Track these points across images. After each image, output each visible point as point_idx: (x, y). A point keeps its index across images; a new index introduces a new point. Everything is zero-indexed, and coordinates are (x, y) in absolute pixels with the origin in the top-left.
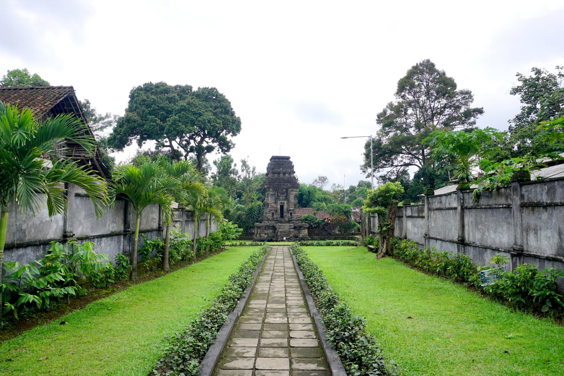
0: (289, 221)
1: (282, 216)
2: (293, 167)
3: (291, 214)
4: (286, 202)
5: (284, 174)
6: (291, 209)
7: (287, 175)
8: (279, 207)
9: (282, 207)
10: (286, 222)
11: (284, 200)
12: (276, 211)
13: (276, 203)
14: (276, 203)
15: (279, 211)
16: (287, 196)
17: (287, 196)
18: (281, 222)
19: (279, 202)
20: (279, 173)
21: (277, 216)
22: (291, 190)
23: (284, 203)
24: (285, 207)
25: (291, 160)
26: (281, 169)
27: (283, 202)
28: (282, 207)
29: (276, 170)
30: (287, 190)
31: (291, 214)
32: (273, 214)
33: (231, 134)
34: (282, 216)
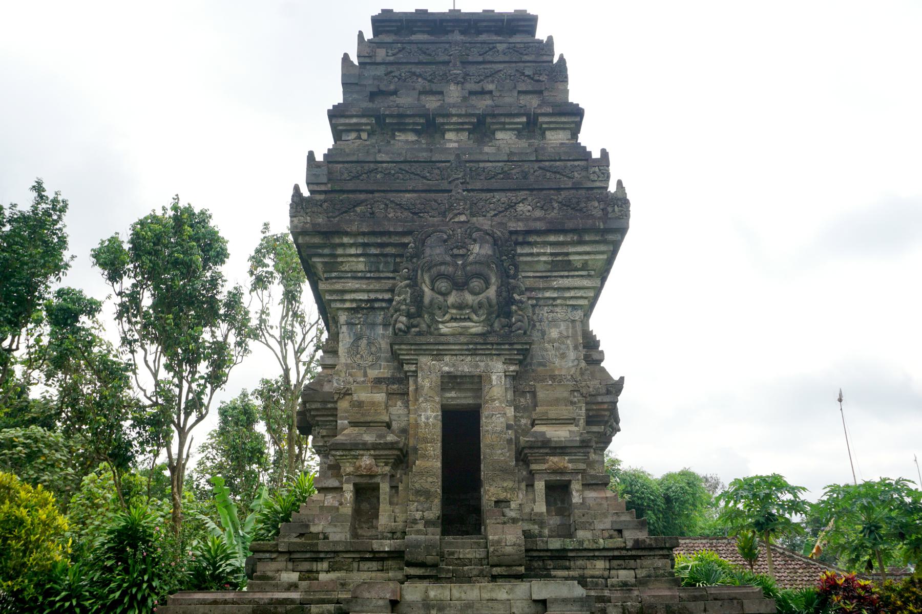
0: (536, 562)
1: (462, 505)
2: (559, 73)
3: (558, 491)
4: (497, 372)
5: (481, 128)
6: (559, 434)
7: (505, 138)
8: (429, 417)
9: (462, 427)
10: (503, 570)
11: (478, 346)
12: (402, 458)
13: (399, 384)
14: (399, 384)
15: (430, 462)
16: (504, 307)
17: (504, 307)
18: (433, 570)
19: (429, 371)
20: (431, 126)
21: (410, 512)
22: (541, 253)
23: (477, 382)
24: (497, 419)
25: (541, 34)
26: (454, 93)
27: (465, 366)
28: (462, 427)
29: (406, 100)
30: (507, 249)
31: (558, 491)
32: (366, 492)
33: (306, 193)
34: (462, 505)
